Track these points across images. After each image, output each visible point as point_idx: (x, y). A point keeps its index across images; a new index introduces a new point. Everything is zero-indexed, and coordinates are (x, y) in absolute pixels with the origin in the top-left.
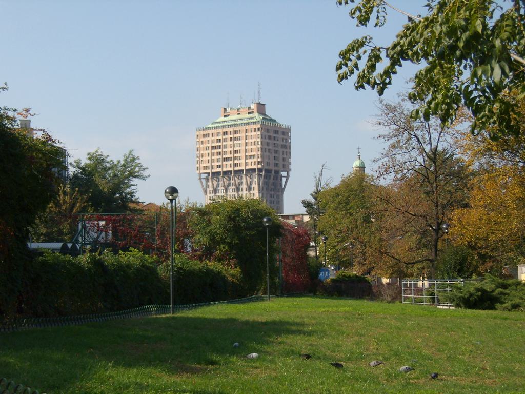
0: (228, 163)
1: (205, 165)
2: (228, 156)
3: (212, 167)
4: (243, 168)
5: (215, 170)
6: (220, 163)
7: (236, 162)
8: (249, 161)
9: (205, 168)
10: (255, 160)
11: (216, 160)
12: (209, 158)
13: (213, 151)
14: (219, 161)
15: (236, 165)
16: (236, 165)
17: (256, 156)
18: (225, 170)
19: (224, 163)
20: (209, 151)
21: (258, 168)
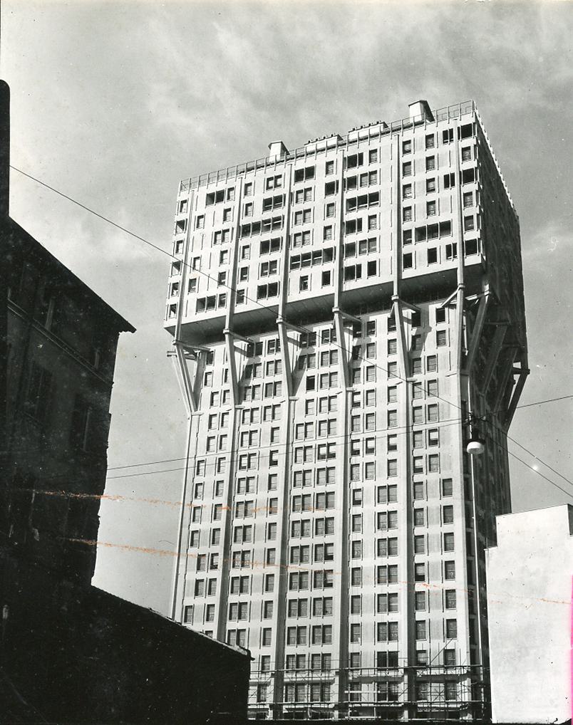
0: (315, 272)
1: (204, 294)
2: (318, 244)
3: (239, 297)
4: (387, 274)
5: (251, 304)
6: (277, 278)
7: (350, 262)
8: (419, 249)
9: (204, 304)
10: (454, 238)
11: (254, 270)
12: (228, 267)
13: (244, 241)
14: (272, 272)
15: (352, 273)
16: (352, 273)
17: (456, 227)
18: (295, 295)
19: (295, 275)
20: (229, 245)
21: (466, 268)
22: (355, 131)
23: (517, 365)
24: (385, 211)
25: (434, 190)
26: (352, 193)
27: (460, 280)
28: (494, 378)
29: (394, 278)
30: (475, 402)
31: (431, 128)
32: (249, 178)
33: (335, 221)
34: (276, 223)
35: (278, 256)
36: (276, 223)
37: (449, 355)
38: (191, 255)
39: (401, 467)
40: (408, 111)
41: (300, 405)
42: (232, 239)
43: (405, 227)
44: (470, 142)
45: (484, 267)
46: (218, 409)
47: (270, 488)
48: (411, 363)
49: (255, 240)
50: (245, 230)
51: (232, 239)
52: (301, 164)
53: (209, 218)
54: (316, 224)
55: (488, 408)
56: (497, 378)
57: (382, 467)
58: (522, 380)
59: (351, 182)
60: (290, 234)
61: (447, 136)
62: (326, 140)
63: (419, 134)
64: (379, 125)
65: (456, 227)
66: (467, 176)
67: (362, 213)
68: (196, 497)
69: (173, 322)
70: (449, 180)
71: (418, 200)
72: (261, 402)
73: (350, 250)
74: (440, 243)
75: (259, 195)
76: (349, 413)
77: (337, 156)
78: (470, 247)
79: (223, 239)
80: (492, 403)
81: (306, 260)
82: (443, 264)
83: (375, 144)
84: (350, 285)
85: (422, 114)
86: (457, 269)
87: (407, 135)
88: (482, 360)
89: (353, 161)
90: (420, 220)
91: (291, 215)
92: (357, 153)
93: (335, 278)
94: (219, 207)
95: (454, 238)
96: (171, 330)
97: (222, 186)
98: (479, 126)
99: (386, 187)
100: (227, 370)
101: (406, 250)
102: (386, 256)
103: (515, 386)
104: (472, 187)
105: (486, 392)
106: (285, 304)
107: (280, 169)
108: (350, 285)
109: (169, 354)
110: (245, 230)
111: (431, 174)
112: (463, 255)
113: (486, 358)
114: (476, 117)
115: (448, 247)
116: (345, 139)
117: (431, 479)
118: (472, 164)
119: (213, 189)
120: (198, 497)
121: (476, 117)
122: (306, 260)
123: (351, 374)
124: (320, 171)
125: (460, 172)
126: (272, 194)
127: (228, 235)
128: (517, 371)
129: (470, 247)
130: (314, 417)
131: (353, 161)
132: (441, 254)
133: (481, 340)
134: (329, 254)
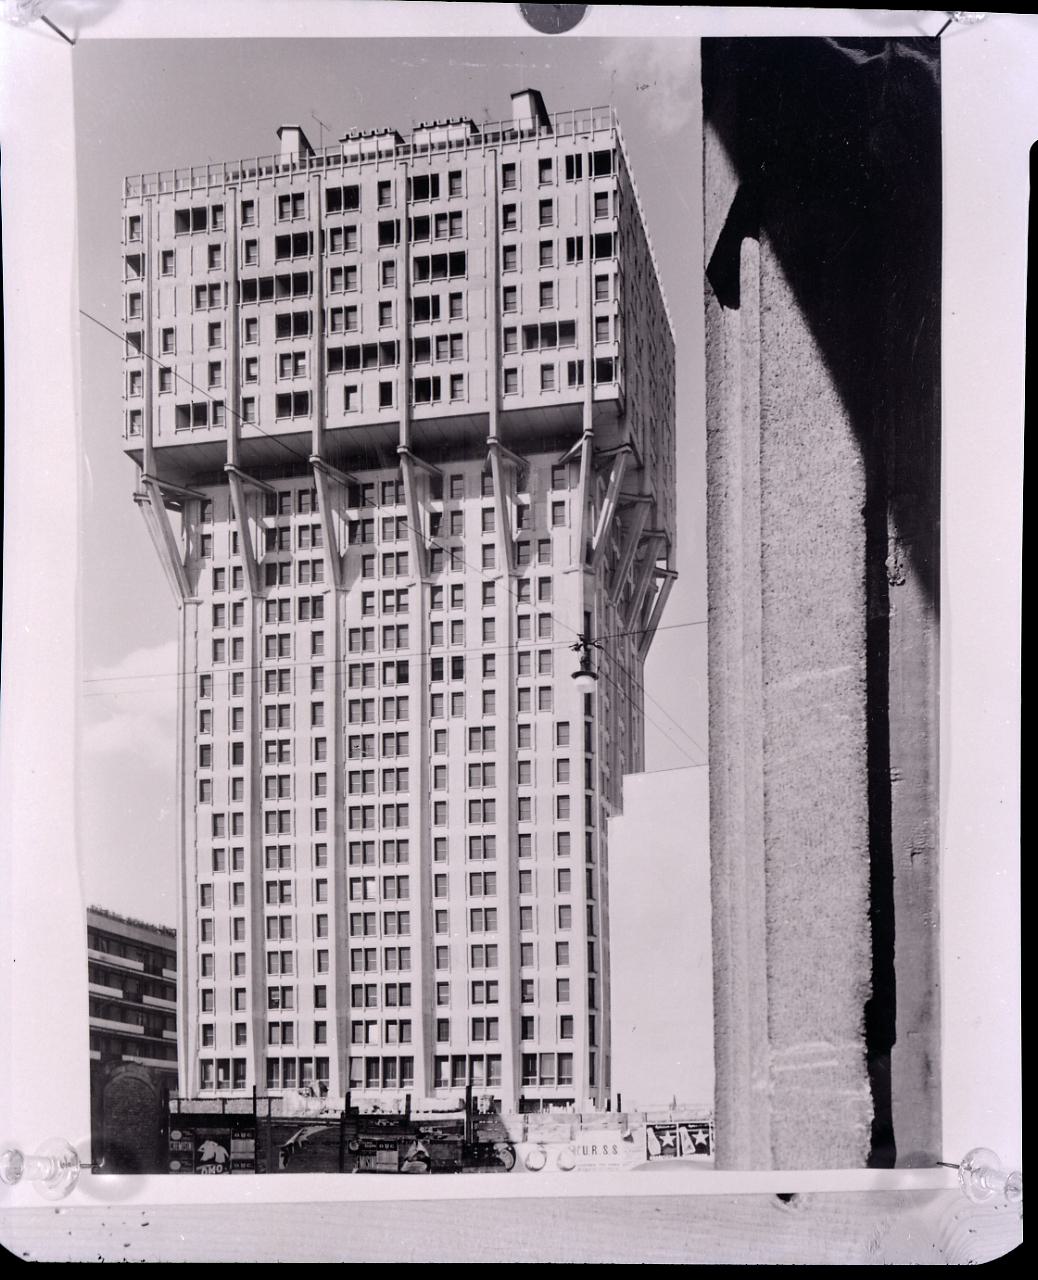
0: (369, 378)
1: (187, 398)
2: (367, 332)
6: (306, 384)
7: (422, 370)
10: (580, 350)
13: (248, 310)
15: (425, 390)
16: (425, 390)
22: (424, 130)
23: (662, 565)
24: (476, 287)
25: (532, 1000)
26: (426, 248)
27: (587, 423)
28: (631, 581)
29: (490, 407)
30: (603, 614)
31: (547, 148)
32: (248, 192)
33: (396, 295)
34: (300, 284)
35: (306, 344)
36: (300, 284)
37: (566, 542)
38: (159, 325)
39: (501, 701)
40: (510, 109)
41: (353, 599)
42: (226, 303)
43: (508, 321)
44: (607, 184)
45: (622, 404)
46: (227, 597)
47: (314, 722)
48: (518, 552)
49: (267, 312)
50: (250, 290)
51: (226, 303)
52: (337, 179)
53: (182, 260)
54: (367, 293)
55: (620, 624)
56: (634, 582)
57: (473, 700)
58: (667, 587)
59: (420, 227)
60: (325, 308)
61: (573, 166)
62: (375, 138)
63: (526, 156)
64: (463, 125)
65: (583, 331)
66: (603, 246)
67: (439, 287)
68: (202, 730)
69: (139, 442)
70: (574, 248)
71: (526, 276)
72: (291, 590)
73: (421, 348)
74: (560, 356)
75: (268, 228)
76: (427, 618)
77: (395, 173)
78: (604, 371)
79: (212, 302)
80: (626, 619)
81: (352, 358)
82: (564, 393)
83: (457, 161)
84: (424, 411)
85: (533, 118)
86: (582, 403)
87: (509, 153)
88: (614, 553)
89: (422, 187)
90: (528, 312)
91: (324, 271)
92: (429, 173)
93: (399, 394)
94: (201, 241)
95: (580, 350)
96: (134, 454)
97: (201, 200)
98: (622, 157)
99: (476, 241)
100: (235, 534)
101: (508, 362)
102: (476, 362)
103: (657, 595)
104: (608, 266)
105: (618, 601)
106: (323, 431)
107: (301, 183)
108: (424, 411)
109: (138, 498)
110: (250, 290)
111: (546, 234)
112: (593, 382)
113: (621, 551)
114: (617, 140)
115: (571, 365)
116: (408, 142)
117: (543, 723)
118: (608, 226)
119: (186, 203)
120: (205, 731)
121: (617, 140)
122: (352, 358)
123: (430, 560)
124: (369, 196)
125: (591, 237)
126: (291, 228)
127: (220, 295)
128: (660, 573)
129: (604, 371)
130: (378, 620)
131: (422, 187)
132: (561, 374)
133: (614, 521)
134: (389, 351)
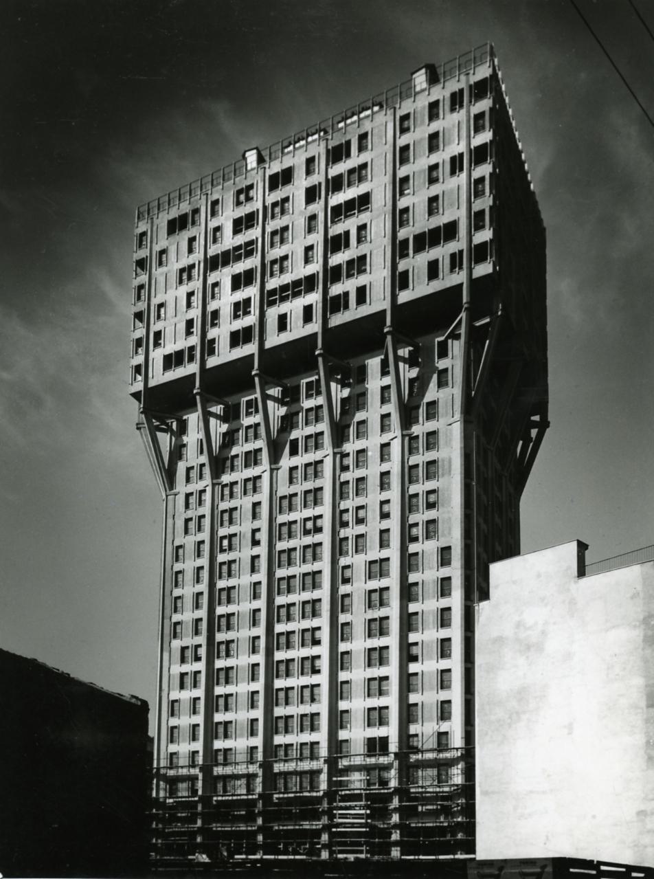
0: (294, 307)
1: (170, 348)
2: (298, 271)
6: (250, 320)
7: (336, 290)
16: (335, 304)
26: (339, 198)
29: (386, 305)
33: (317, 238)
34: (247, 250)
35: (252, 292)
36: (247, 250)
41: (283, 474)
42: (199, 276)
43: (402, 234)
46: (195, 487)
48: (408, 416)
49: (224, 276)
51: (199, 276)
54: (294, 247)
57: (373, 539)
66: (479, 155)
67: (349, 225)
70: (456, 164)
73: (334, 274)
74: (442, 252)
84: (337, 320)
86: (462, 284)
89: (337, 154)
97: (185, 207)
100: (201, 440)
102: (377, 277)
104: (485, 170)
110: (213, 263)
111: (434, 158)
118: (486, 137)
119: (174, 213)
123: (340, 434)
125: (471, 150)
127: (195, 272)
129: (479, 253)
130: (300, 487)
134: (309, 283)
